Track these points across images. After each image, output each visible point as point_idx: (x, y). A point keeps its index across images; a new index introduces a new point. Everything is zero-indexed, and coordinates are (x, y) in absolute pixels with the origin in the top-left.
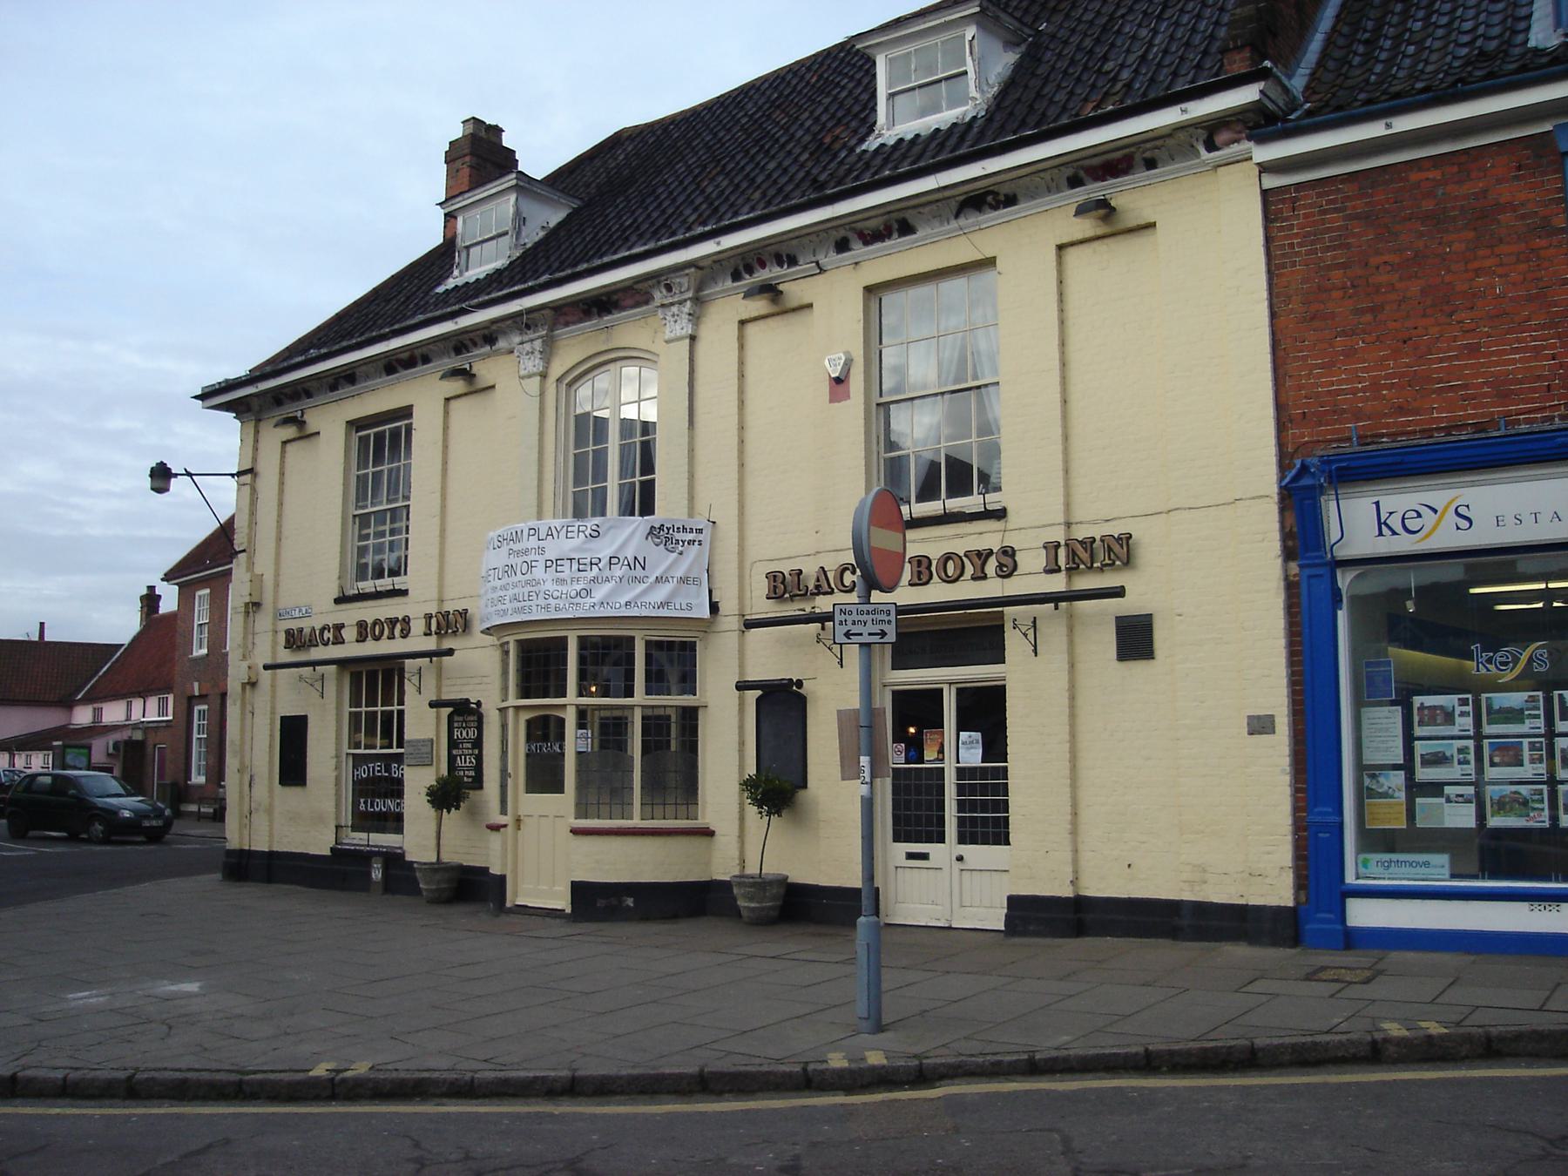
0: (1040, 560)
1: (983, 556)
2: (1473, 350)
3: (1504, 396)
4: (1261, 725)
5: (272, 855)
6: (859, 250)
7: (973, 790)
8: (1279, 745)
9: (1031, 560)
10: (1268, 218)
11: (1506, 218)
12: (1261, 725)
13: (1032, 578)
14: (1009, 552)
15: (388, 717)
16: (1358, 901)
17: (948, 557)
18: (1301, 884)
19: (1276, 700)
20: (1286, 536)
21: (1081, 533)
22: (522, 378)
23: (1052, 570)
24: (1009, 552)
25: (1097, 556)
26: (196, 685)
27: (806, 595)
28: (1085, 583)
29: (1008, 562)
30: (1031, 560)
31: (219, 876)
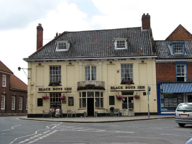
0: (64, 89)
1: (59, 88)
2: (169, 76)
3: (171, 79)
4: (155, 100)
5: (36, 114)
6: (120, 61)
7: (132, 106)
8: (156, 102)
9: (136, 88)
10: (156, 65)
11: (172, 68)
12: (155, 100)
13: (136, 89)
14: (62, 88)
15: (101, 99)
16: (155, 112)
17: (129, 87)
18: (158, 111)
19: (156, 99)
20: (157, 87)
21: (141, 86)
22: (31, 69)
23: (138, 88)
24: (62, 88)
25: (141, 87)
26: (15, 93)
27: (42, 90)
28: (68, 91)
29: (61, 89)
30: (136, 88)
31: (27, 117)
